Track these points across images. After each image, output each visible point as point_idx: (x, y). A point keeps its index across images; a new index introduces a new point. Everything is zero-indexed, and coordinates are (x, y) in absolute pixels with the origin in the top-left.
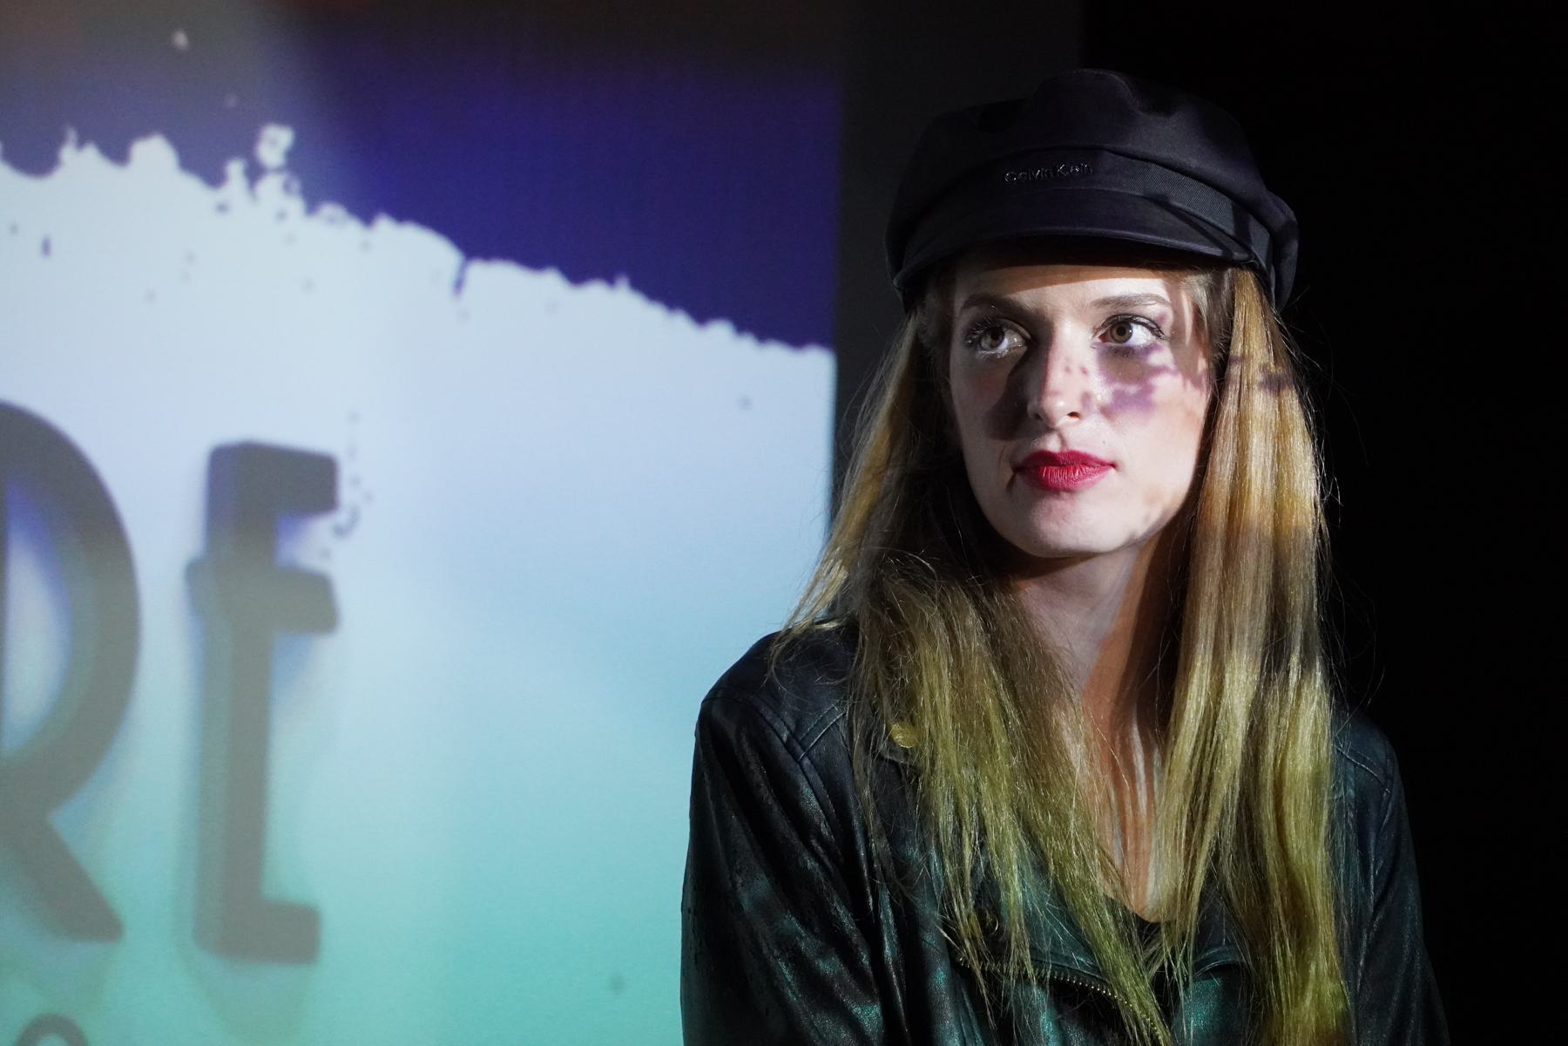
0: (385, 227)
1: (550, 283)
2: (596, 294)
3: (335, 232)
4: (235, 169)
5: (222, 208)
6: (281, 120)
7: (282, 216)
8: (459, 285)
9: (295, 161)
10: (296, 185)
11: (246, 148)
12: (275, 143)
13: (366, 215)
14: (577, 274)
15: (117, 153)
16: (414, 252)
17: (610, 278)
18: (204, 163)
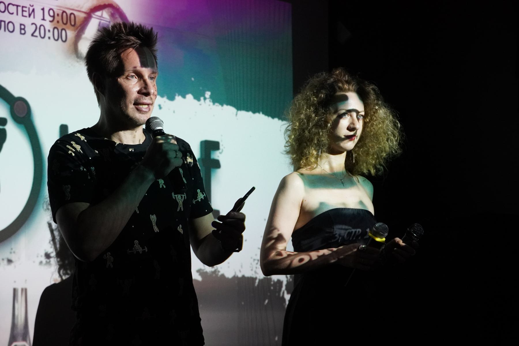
0: (225, 106)
1: (250, 113)
2: (257, 114)
3: (217, 107)
4: (202, 98)
5: (200, 105)
7: (209, 105)
8: (236, 114)
9: (211, 97)
12: (208, 94)
13: (222, 105)
14: (254, 112)
15: (184, 97)
16: (230, 110)
17: (259, 113)
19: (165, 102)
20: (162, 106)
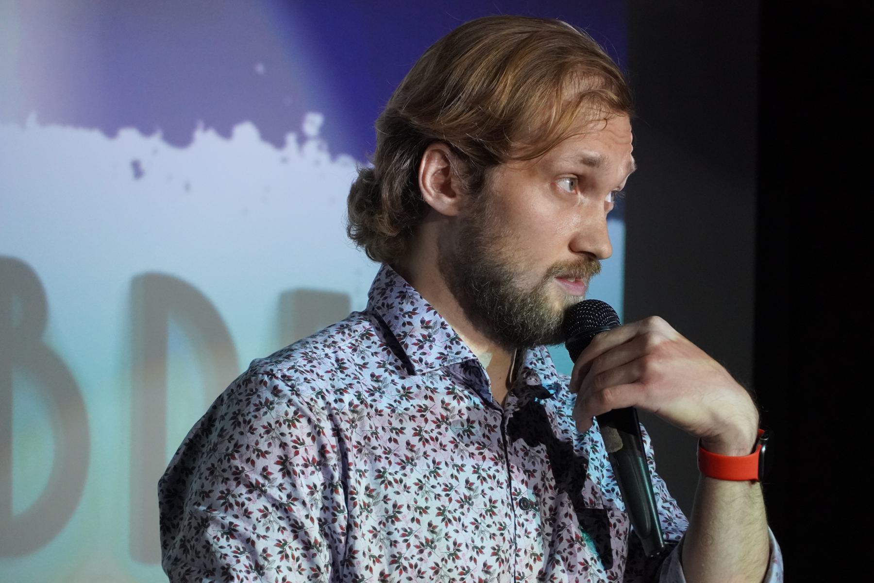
4: (291, 138)
5: (284, 160)
6: (316, 109)
7: (317, 163)
9: (325, 133)
10: (325, 146)
11: (297, 126)
12: (313, 123)
15: (226, 132)
18: (273, 136)
19: (155, 152)
20: (144, 166)
